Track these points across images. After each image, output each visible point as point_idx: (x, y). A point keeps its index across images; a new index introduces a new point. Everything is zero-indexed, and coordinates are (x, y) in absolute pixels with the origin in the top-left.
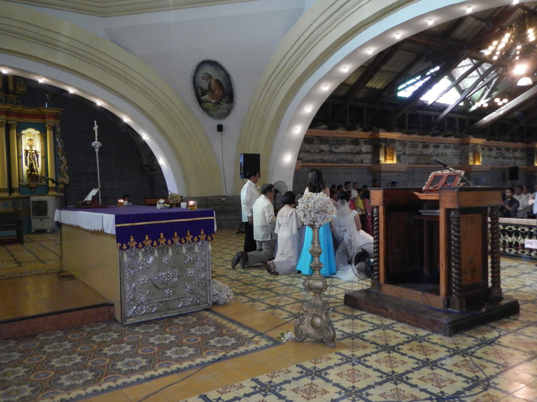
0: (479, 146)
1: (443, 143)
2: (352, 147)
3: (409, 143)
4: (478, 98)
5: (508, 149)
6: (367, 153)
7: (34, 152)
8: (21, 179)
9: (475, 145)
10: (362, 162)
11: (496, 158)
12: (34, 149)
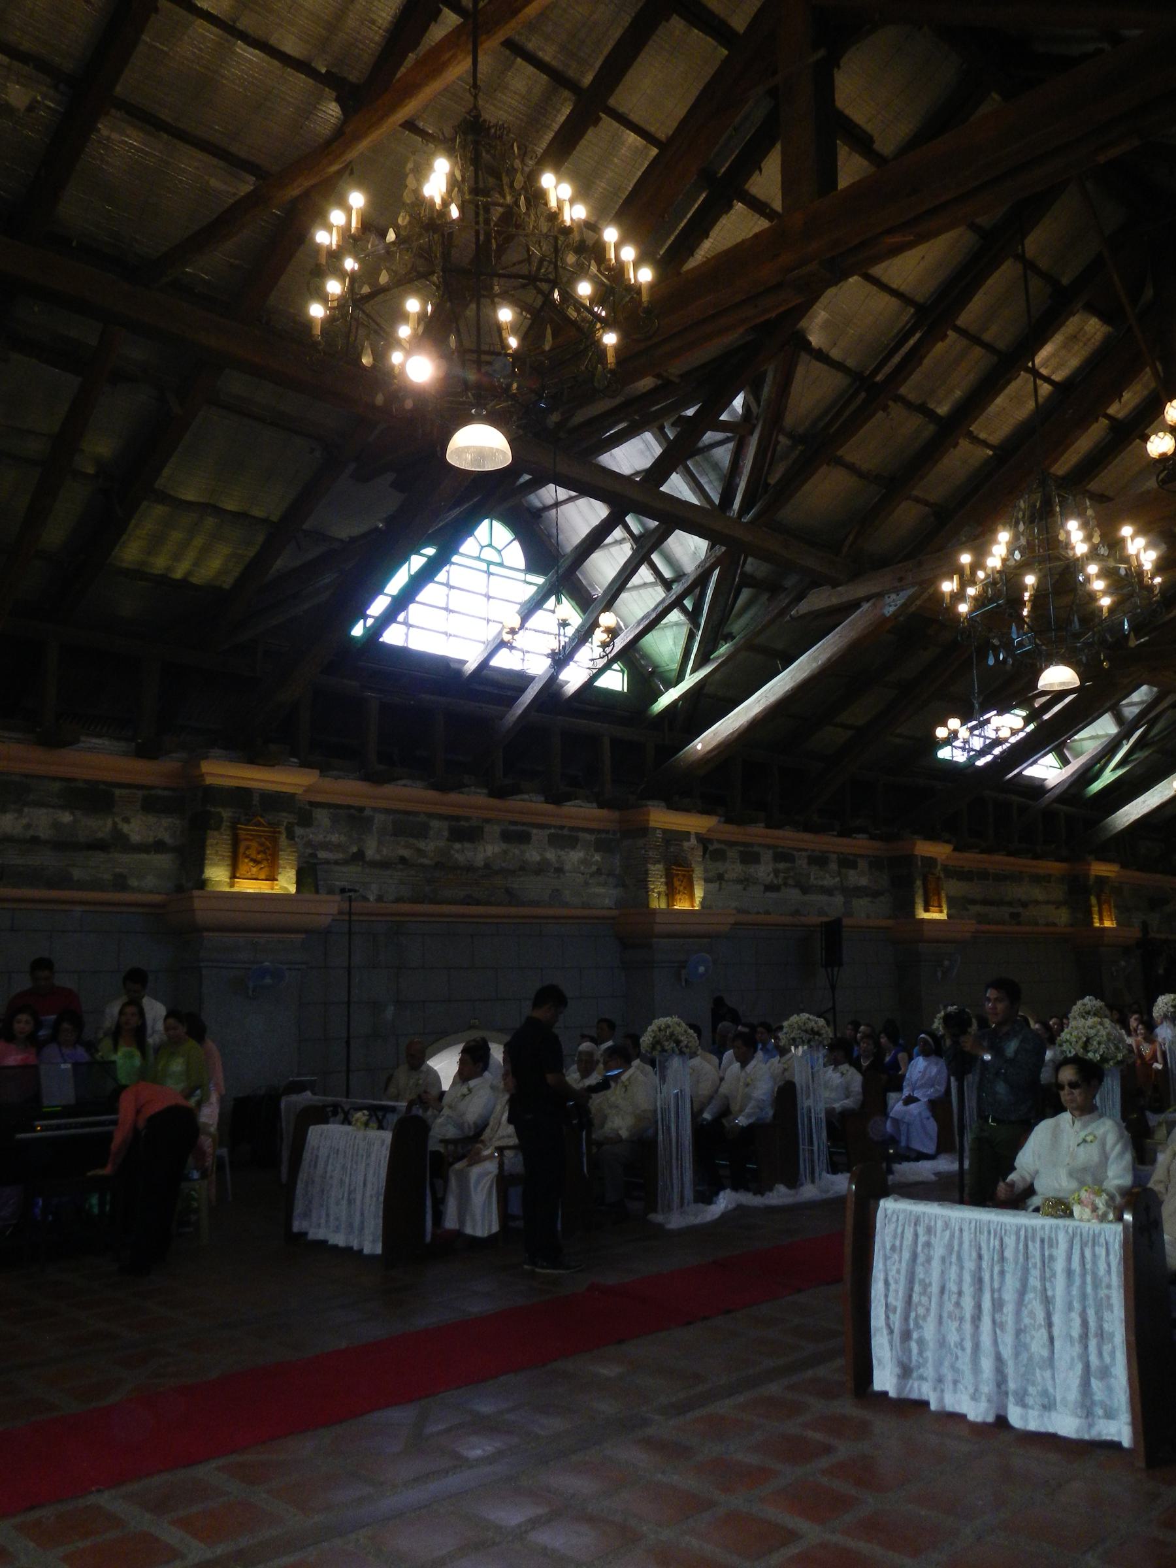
0: (693, 841)
1: (548, 827)
2: (66, 818)
3: (379, 818)
4: (675, 666)
5: (820, 860)
6: (159, 846)
9: (674, 837)
10: (120, 883)
11: (769, 888)
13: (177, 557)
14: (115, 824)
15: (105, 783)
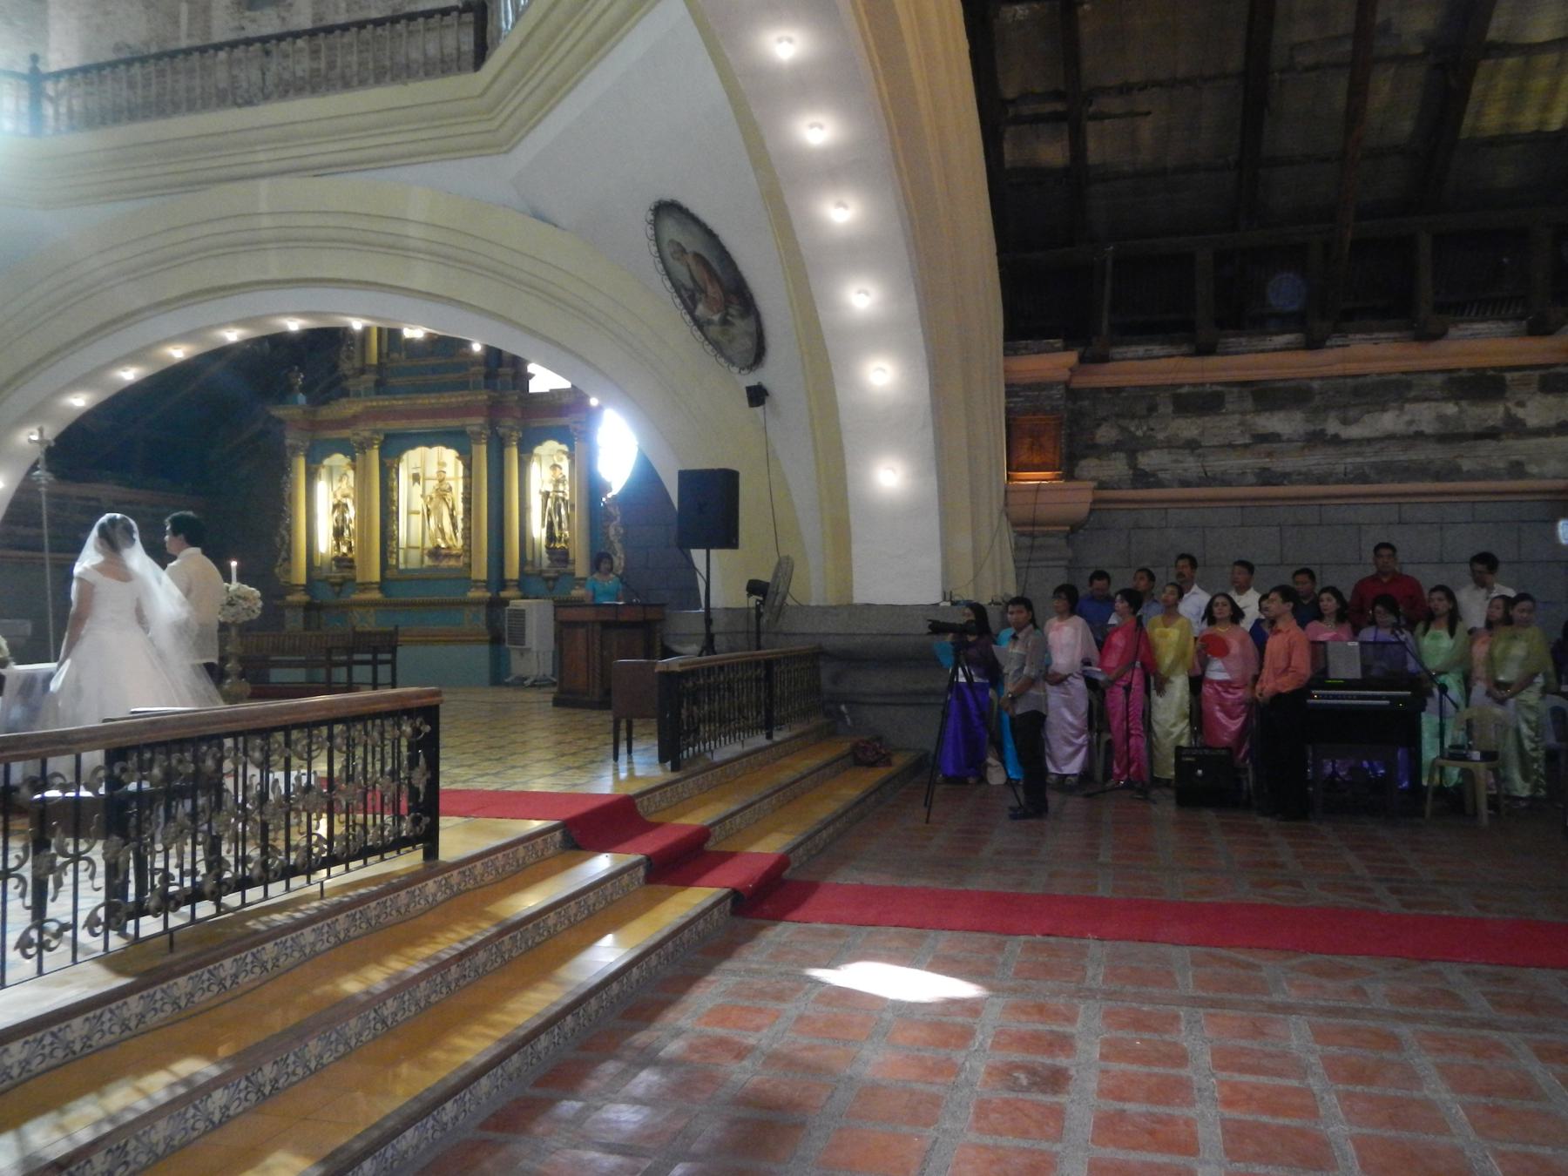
2: (1450, 409)
8: (529, 558)
13: (1546, 107)
14: (1507, 410)
15: (1494, 368)
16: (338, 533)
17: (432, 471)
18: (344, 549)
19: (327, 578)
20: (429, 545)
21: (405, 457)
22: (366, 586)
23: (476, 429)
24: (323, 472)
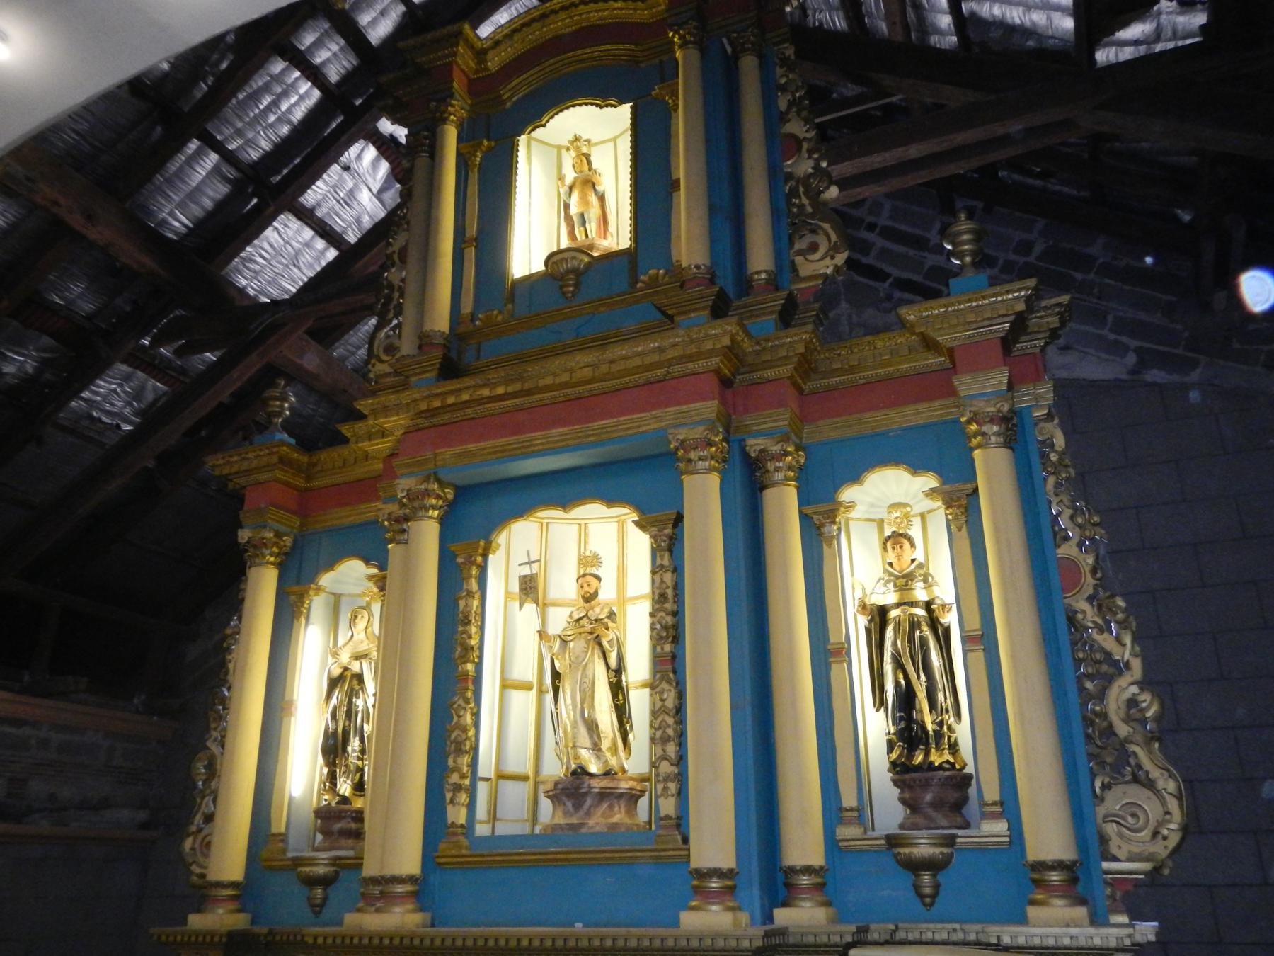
7: (921, 612)
8: (849, 799)
12: (920, 594)
16: (334, 748)
17: (563, 584)
18: (345, 788)
19: (298, 862)
20: (554, 769)
21: (501, 538)
22: (381, 890)
23: (698, 432)
24: (317, 605)
